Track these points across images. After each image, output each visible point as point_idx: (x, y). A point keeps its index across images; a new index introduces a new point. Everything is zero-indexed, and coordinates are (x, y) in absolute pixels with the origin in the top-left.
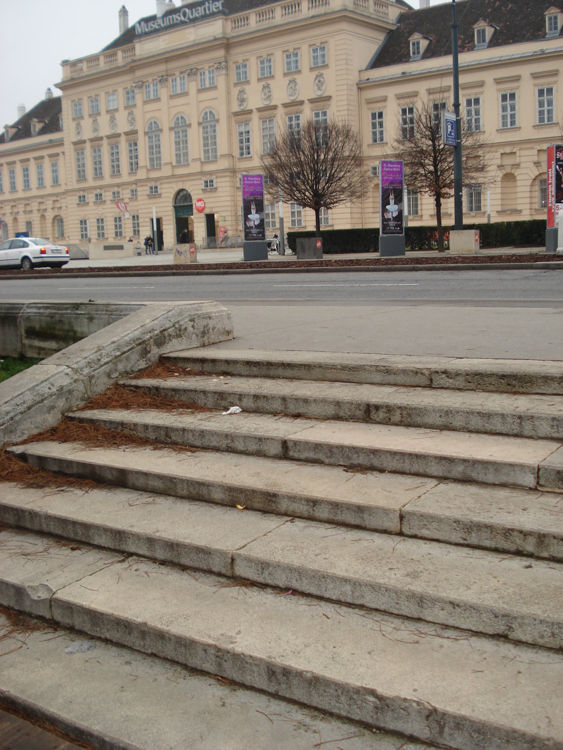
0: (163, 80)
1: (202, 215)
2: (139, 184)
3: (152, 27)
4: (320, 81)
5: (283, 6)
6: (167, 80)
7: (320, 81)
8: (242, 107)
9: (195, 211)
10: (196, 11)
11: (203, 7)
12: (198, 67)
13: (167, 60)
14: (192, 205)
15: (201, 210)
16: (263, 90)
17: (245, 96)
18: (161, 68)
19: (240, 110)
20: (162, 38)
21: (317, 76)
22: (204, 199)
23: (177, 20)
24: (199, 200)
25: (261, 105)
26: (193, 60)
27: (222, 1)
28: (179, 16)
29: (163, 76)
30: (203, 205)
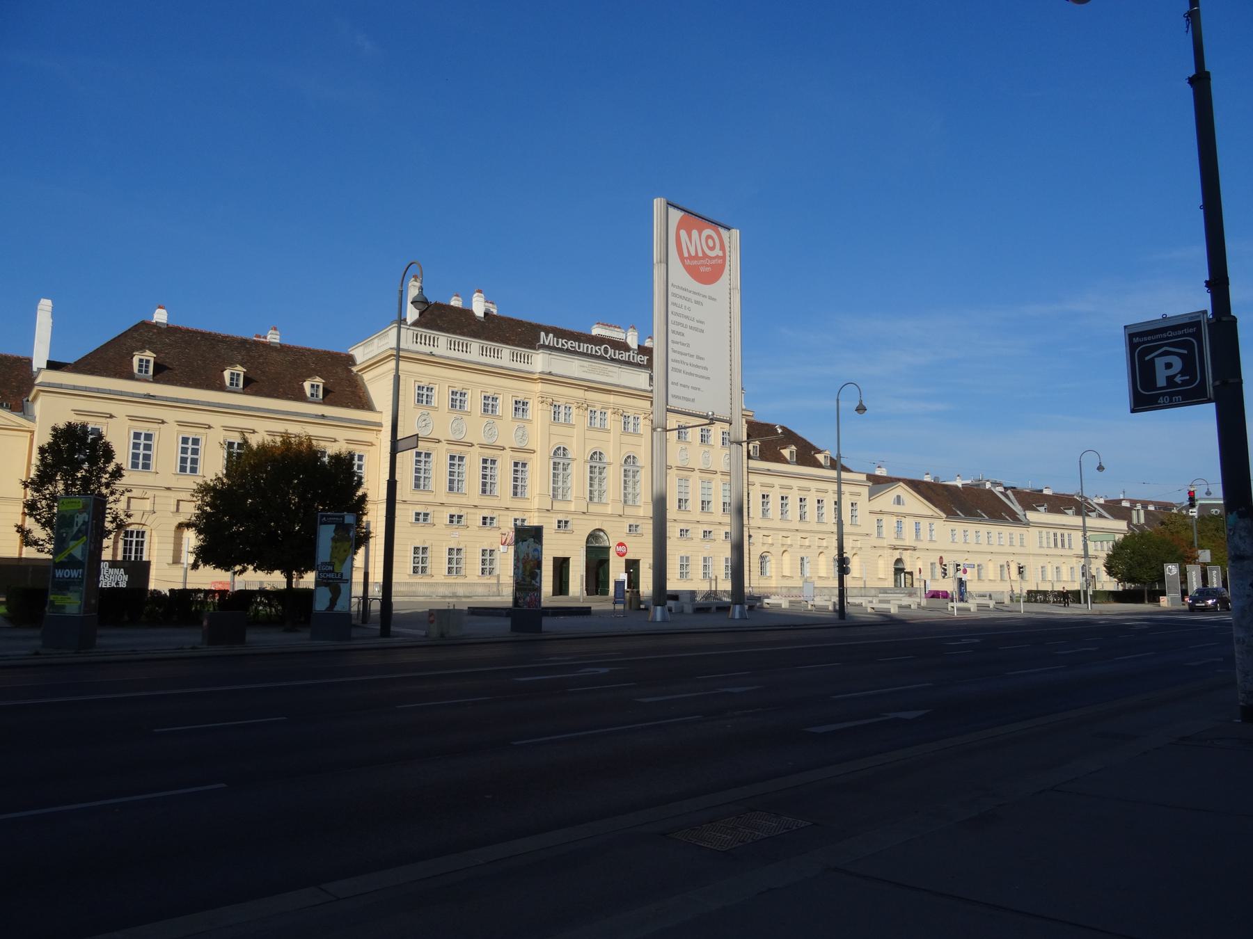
10: (619, 354)
15: (621, 555)
23: (596, 351)
24: (621, 544)
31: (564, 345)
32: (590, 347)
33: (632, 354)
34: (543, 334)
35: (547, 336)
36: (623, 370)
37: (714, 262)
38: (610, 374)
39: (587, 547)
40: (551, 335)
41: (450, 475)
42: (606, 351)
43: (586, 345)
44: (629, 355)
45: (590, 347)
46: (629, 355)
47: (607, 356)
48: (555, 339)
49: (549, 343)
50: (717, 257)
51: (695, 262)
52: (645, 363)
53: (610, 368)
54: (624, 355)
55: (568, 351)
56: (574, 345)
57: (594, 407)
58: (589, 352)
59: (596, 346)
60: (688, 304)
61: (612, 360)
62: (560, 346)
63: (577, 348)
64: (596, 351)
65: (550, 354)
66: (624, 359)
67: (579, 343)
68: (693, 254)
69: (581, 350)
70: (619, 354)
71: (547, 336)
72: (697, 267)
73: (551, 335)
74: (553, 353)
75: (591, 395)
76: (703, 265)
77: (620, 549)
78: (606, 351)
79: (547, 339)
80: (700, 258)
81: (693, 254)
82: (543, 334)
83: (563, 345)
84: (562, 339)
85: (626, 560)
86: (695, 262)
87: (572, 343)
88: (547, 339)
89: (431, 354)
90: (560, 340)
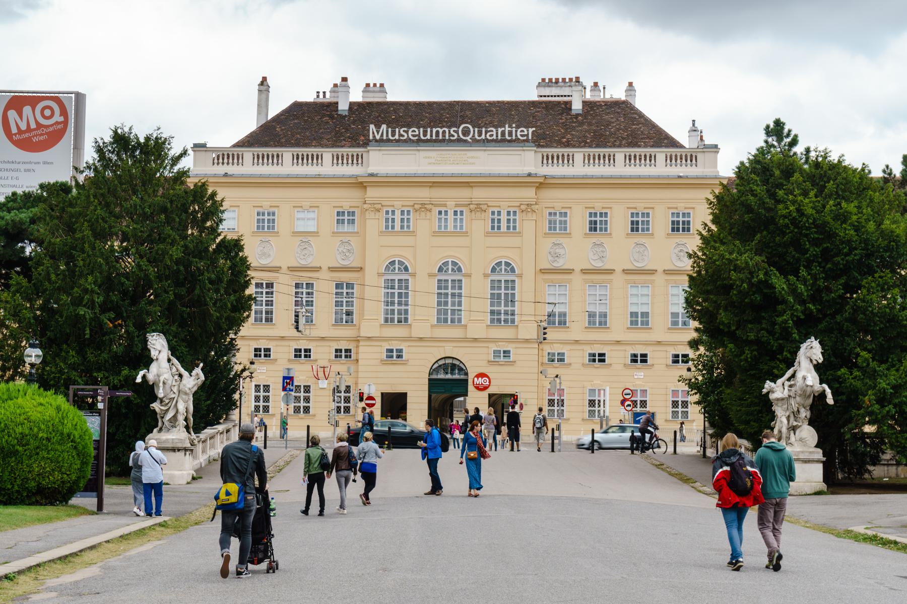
0: (423, 207)
1: (485, 394)
2: (361, 343)
3: (400, 135)
5: (628, 154)
6: (430, 211)
8: (555, 264)
9: (471, 388)
10: (486, 132)
11: (500, 130)
12: (490, 204)
13: (434, 185)
14: (467, 380)
17: (561, 251)
18: (423, 194)
19: (549, 267)
20: (423, 154)
22: (489, 375)
26: (479, 194)
27: (534, 129)
28: (457, 132)
30: (488, 383)
31: (403, 136)
32: (441, 131)
33: (507, 129)
34: (372, 127)
35: (378, 127)
37: (51, 129)
38: (470, 160)
39: (430, 380)
40: (384, 127)
42: (466, 132)
43: (434, 130)
44: (503, 133)
46: (503, 133)
47: (468, 138)
48: (390, 130)
50: (57, 123)
51: (27, 135)
52: (530, 137)
53: (470, 154)
54: (494, 133)
55: (408, 141)
56: (417, 133)
57: (445, 206)
58: (441, 137)
59: (449, 127)
60: (15, 174)
61: (475, 141)
62: (397, 137)
66: (494, 137)
67: (424, 127)
68: (23, 127)
69: (428, 137)
70: (486, 132)
71: (378, 127)
72: (30, 138)
73: (384, 127)
76: (36, 136)
77: (480, 381)
79: (378, 133)
80: (34, 130)
81: (23, 127)
82: (372, 127)
83: (400, 135)
85: (490, 396)
86: (27, 135)
88: (378, 133)
89: (226, 175)
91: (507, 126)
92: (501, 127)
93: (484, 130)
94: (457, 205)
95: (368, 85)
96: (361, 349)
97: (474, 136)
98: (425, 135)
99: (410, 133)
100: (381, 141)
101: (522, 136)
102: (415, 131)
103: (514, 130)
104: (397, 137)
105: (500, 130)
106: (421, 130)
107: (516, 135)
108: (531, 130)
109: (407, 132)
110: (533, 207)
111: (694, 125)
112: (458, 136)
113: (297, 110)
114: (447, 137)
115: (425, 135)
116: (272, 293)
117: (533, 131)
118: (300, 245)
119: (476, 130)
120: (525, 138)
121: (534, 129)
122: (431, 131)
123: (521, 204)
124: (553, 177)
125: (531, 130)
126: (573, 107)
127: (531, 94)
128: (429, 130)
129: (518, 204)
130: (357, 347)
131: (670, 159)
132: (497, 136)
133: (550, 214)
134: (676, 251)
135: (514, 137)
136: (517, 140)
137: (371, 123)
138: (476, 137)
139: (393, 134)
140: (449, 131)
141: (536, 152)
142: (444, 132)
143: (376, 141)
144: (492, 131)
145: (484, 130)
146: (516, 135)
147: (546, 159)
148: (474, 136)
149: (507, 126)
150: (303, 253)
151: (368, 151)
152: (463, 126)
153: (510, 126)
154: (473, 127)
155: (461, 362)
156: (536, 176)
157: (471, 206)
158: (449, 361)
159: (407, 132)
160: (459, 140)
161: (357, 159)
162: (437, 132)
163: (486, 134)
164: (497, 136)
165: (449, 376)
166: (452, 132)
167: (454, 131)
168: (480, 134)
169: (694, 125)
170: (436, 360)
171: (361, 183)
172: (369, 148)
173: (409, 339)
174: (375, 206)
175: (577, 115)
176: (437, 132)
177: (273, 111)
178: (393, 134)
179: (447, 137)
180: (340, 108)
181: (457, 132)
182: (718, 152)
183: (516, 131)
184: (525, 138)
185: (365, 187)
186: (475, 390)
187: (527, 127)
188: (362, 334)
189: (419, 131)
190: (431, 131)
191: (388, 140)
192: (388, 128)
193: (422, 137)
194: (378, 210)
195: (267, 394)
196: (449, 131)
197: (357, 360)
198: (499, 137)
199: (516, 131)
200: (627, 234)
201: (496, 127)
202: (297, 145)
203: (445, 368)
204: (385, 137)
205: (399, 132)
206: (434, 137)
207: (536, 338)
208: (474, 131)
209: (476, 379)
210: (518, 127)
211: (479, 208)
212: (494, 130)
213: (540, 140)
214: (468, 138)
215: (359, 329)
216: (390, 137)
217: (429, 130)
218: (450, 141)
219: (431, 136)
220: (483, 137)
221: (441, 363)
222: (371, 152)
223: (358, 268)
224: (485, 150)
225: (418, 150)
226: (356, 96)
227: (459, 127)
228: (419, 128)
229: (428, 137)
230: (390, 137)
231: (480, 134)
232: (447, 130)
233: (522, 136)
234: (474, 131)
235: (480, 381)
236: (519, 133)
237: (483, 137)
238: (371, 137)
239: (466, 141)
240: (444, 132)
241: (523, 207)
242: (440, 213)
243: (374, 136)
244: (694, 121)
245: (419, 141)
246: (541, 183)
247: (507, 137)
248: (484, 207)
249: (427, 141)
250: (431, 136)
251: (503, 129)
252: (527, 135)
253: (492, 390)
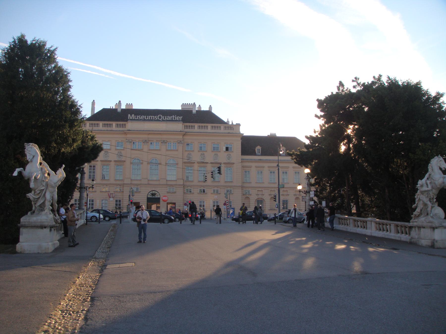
1: (166, 203)
3: (138, 118)
4: (229, 157)
6: (148, 142)
7: (229, 157)
9: (161, 201)
10: (167, 118)
11: (171, 117)
12: (168, 140)
14: (159, 198)
16: (201, 155)
17: (191, 156)
18: (146, 136)
21: (228, 155)
23: (155, 118)
25: (199, 161)
26: (164, 137)
27: (182, 117)
28: (157, 117)
29: (146, 140)
32: (152, 117)
33: (173, 117)
34: (129, 115)
35: (131, 115)
36: (168, 124)
40: (133, 115)
41: (89, 173)
42: (160, 118)
43: (150, 117)
44: (172, 118)
45: (152, 117)
46: (172, 118)
47: (161, 119)
48: (135, 116)
49: (132, 118)
52: (181, 119)
54: (169, 118)
56: (144, 117)
59: (155, 116)
61: (163, 120)
63: (146, 119)
64: (155, 118)
65: (132, 122)
66: (169, 119)
69: (148, 119)
71: (131, 115)
73: (133, 115)
74: (133, 122)
75: (150, 136)
78: (160, 118)
79: (131, 117)
82: (129, 115)
83: (138, 118)
84: (138, 116)
85: (167, 203)
87: (143, 117)
88: (131, 117)
90: (137, 116)
91: (173, 116)
92: (171, 116)
93: (166, 117)
94: (157, 141)
95: (127, 104)
96: (125, 188)
97: (162, 119)
98: (147, 118)
99: (142, 117)
100: (132, 120)
101: (178, 119)
102: (143, 117)
103: (176, 117)
104: (137, 118)
105: (171, 117)
106: (145, 116)
107: (176, 119)
108: (181, 117)
109: (141, 117)
110: (182, 142)
111: (228, 120)
112: (158, 119)
113: (104, 111)
114: (154, 119)
115: (147, 118)
116: (95, 169)
117: (182, 118)
118: (104, 153)
119: (163, 117)
120: (179, 120)
121: (182, 117)
122: (149, 117)
123: (178, 141)
124: (188, 132)
125: (181, 117)
126: (193, 112)
127: (180, 108)
128: (148, 116)
129: (177, 141)
130: (123, 187)
131: (225, 128)
132: (170, 119)
133: (187, 144)
134: (228, 157)
135: (176, 119)
136: (177, 121)
137: (129, 114)
138: (163, 119)
139: (136, 118)
140: (155, 117)
141: (183, 124)
142: (153, 118)
143: (130, 120)
144: (168, 117)
145: (166, 117)
146: (176, 119)
147: (186, 127)
148: (162, 119)
149: (173, 116)
150: (106, 156)
151: (128, 123)
152: (159, 115)
153: (174, 116)
154: (163, 116)
155: (158, 192)
156: (183, 131)
157: (162, 141)
158: (154, 192)
159: (141, 117)
160: (158, 120)
161: (124, 126)
162: (151, 117)
163: (166, 118)
164: (170, 119)
165: (154, 197)
166: (155, 117)
167: (156, 117)
168: (164, 118)
169: (228, 120)
170: (149, 192)
171: (125, 133)
172: (128, 122)
173: (140, 184)
174: (130, 141)
175: (195, 114)
176: (151, 117)
177: (96, 111)
178: (136, 118)
179: (154, 119)
180: (118, 110)
181: (157, 117)
182: (240, 126)
183: (176, 118)
184: (179, 120)
185: (127, 134)
186: (163, 201)
187: (180, 116)
188: (125, 183)
189: (145, 117)
190: (149, 117)
191: (134, 120)
192: (134, 115)
193: (146, 119)
194: (131, 142)
195: (93, 203)
196: (155, 117)
197: (123, 192)
198: (171, 119)
199: (176, 118)
200: (212, 151)
201: (170, 116)
202: (104, 121)
203: (153, 194)
204: (133, 119)
205: (138, 117)
206: (149, 119)
207: (183, 184)
208: (163, 117)
209: (163, 197)
210: (177, 116)
211: (164, 142)
212: (169, 117)
213: (184, 121)
214: (161, 119)
215: (124, 181)
216: (135, 118)
217: (148, 116)
218: (155, 120)
219: (149, 118)
220: (166, 119)
221: (151, 192)
222: (129, 123)
223: (124, 161)
224: (166, 123)
225: (144, 123)
226: (123, 107)
227: (157, 116)
228: (144, 116)
229: (148, 119)
230: (135, 118)
231: (164, 118)
232: (154, 117)
233: (178, 119)
234: (163, 117)
235: (164, 198)
236: (177, 118)
237: (166, 119)
238: (129, 118)
239: (160, 120)
240: (153, 118)
241: (179, 142)
242: (151, 143)
243: (130, 118)
244: (228, 119)
245: (145, 120)
246: (184, 134)
247: (173, 119)
248: (166, 141)
249: (147, 120)
250: (149, 118)
251: (172, 117)
252: (180, 119)
253: (168, 201)
